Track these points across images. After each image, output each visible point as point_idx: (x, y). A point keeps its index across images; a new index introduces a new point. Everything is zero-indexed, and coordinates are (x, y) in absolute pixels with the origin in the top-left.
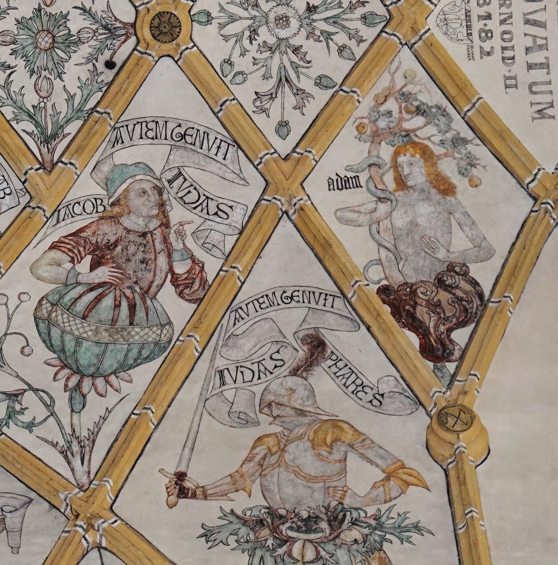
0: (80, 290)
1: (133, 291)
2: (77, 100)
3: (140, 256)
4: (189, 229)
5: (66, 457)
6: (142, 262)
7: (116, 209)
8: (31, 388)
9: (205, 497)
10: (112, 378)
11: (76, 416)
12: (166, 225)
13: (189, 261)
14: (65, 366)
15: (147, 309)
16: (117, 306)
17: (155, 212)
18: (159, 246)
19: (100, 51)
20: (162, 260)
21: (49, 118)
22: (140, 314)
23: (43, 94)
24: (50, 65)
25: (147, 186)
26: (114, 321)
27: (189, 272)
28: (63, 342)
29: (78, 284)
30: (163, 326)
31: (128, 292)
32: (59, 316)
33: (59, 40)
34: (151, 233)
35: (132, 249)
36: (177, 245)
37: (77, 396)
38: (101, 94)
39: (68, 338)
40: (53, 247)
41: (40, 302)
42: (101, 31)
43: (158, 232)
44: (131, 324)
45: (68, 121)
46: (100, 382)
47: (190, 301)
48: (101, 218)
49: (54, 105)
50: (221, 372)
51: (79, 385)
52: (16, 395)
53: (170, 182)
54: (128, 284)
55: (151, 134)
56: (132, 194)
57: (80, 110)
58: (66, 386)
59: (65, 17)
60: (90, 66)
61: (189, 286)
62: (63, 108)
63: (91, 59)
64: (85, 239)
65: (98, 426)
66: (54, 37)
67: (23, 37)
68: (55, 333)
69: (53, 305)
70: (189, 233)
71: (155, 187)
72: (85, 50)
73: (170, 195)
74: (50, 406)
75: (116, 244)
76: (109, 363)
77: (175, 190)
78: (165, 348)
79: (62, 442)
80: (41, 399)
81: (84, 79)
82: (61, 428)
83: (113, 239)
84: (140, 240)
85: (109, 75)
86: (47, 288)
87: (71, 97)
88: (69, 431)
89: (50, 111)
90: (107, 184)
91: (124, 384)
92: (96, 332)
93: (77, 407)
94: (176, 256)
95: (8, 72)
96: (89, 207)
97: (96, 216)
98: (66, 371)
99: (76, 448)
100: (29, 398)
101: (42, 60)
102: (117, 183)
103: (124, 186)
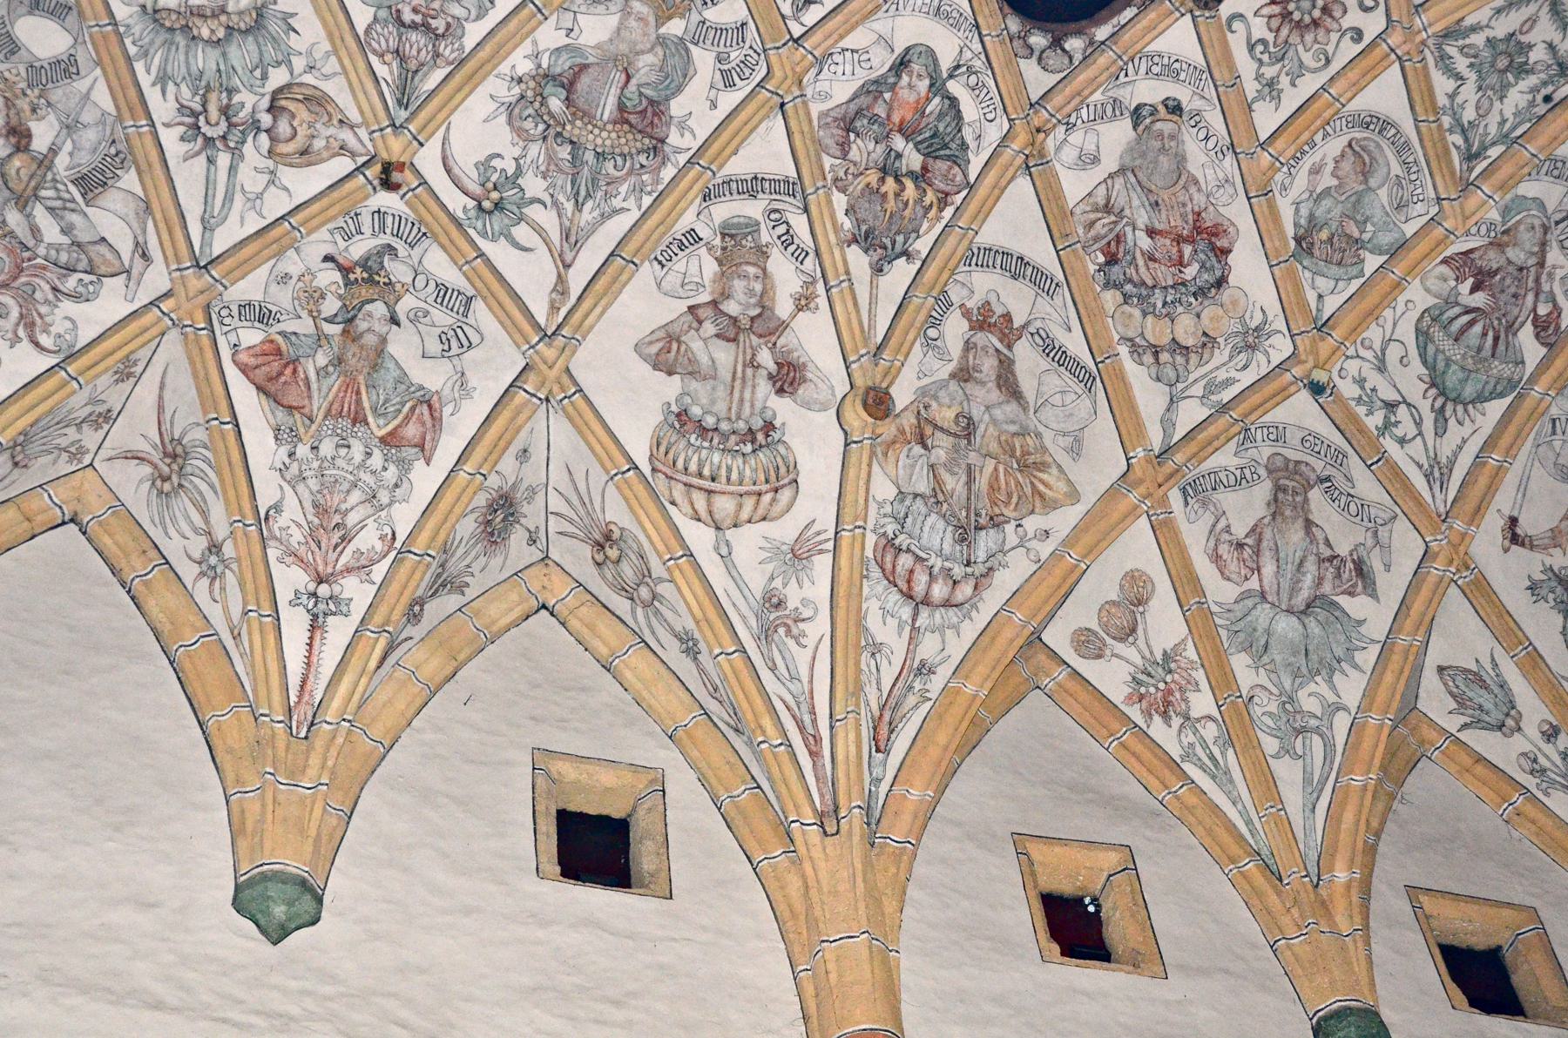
0: (1457, 310)
1: (1500, 323)
2: (1508, 125)
3: (1513, 290)
4: (1559, 273)
5: (1429, 481)
6: (1515, 296)
7: (1505, 238)
8: (1405, 401)
9: (1532, 547)
10: (1470, 407)
11: (1438, 440)
12: (1541, 264)
13: (1550, 305)
14: (1433, 385)
15: (1508, 343)
16: (1485, 334)
17: (1536, 249)
18: (1531, 284)
19: (1545, 84)
20: (1530, 298)
21: (1478, 137)
22: (1501, 347)
23: (1481, 112)
24: (1497, 87)
25: (1537, 222)
26: (1479, 350)
27: (1548, 315)
28: (1435, 361)
29: (1457, 304)
30: (1517, 364)
31: (1496, 323)
32: (1437, 334)
33: (1516, 65)
34: (1528, 268)
35: (1508, 281)
36: (1546, 287)
37: (1441, 420)
38: (1529, 125)
39: (1440, 357)
40: (1445, 261)
41: (1424, 312)
42: (1555, 67)
43: (1533, 270)
44: (1493, 356)
45: (1494, 144)
46: (1460, 408)
47: (1542, 344)
48: (1491, 243)
49: (1486, 125)
50: (1554, 421)
51: (1443, 406)
52: (1393, 406)
53: (1557, 223)
54: (1497, 315)
55: (1556, 173)
56: (1522, 228)
57: (1506, 136)
58: (1433, 405)
59: (1530, 47)
60: (1530, 97)
61: (1545, 329)
62: (1493, 130)
63: (1534, 90)
64: (1473, 260)
65: (1456, 455)
66: (1512, 61)
67: (1486, 54)
68: (1431, 349)
69: (1433, 320)
70: (1558, 278)
71: (1543, 225)
72: (1533, 80)
73: (1552, 237)
74: (1418, 424)
75: (1496, 272)
76: (1469, 391)
77: (1558, 232)
78: (1515, 387)
79: (1426, 466)
80: (1412, 415)
81: (1520, 107)
82: (1426, 450)
83: (1495, 266)
84: (1515, 273)
85: (1542, 109)
86: (1431, 301)
87: (1504, 121)
88: (1432, 454)
89: (1481, 130)
90: (1506, 212)
91: (1479, 416)
92: (1464, 356)
93: (1440, 431)
94: (1542, 297)
95: (1459, 83)
96: (1483, 230)
97: (1487, 240)
98: (1433, 391)
99: (1437, 475)
100: (1402, 411)
101: (1493, 79)
102: (1513, 213)
103: (1518, 218)
